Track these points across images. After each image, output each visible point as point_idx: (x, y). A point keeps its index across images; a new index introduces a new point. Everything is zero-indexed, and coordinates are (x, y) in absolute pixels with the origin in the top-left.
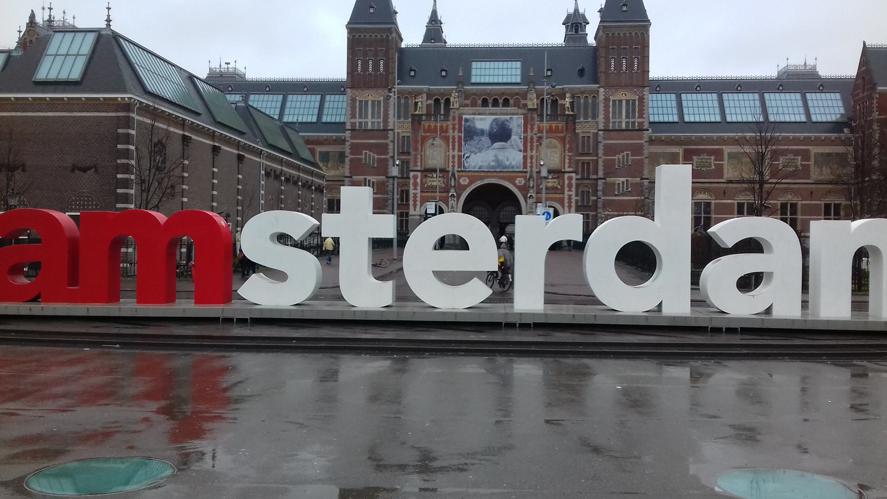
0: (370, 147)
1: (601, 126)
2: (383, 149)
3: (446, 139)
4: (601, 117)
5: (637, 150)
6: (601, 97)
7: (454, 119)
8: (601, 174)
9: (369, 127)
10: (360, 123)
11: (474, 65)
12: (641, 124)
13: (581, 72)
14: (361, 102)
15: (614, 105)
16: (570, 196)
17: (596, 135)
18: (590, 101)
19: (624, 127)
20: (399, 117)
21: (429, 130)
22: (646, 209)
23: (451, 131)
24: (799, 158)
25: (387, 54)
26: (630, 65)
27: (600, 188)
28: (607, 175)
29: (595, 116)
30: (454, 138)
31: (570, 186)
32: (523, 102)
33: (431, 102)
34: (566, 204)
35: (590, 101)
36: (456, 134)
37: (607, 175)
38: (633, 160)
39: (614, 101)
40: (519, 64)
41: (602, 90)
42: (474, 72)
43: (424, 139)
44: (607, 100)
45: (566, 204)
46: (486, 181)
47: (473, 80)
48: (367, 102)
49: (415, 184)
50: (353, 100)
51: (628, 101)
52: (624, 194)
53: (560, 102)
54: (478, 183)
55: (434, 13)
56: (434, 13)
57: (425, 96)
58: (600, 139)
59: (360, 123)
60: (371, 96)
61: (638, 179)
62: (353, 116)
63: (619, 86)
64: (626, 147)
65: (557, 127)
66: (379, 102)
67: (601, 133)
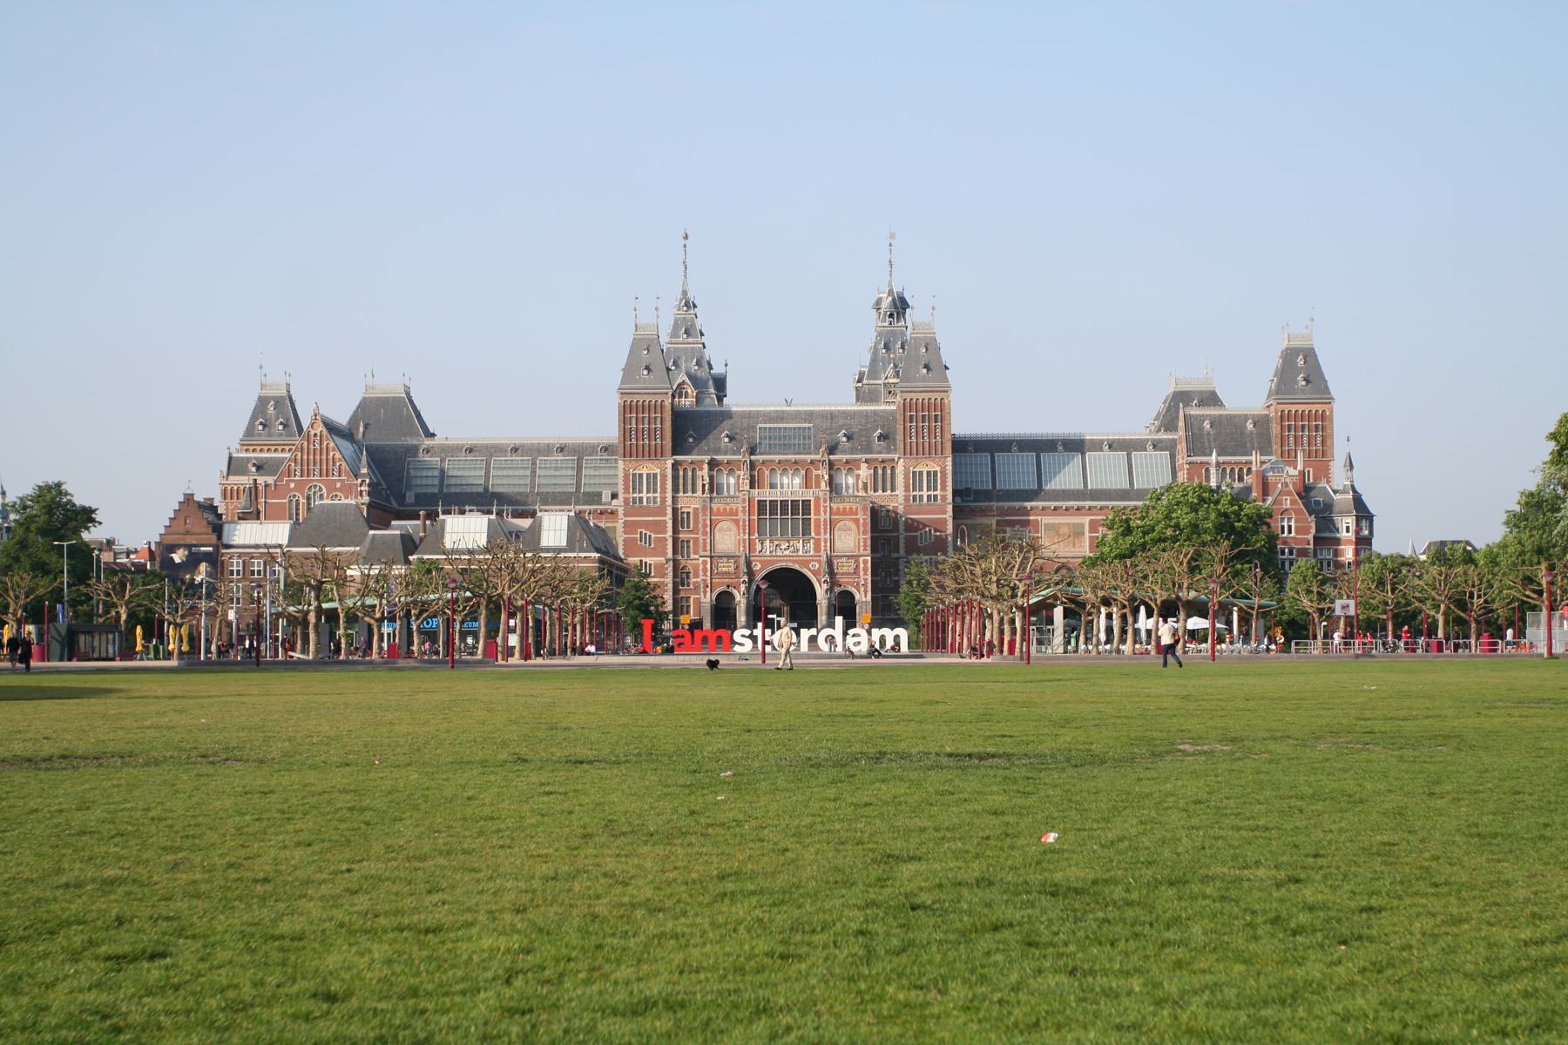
0: (647, 525)
1: (901, 499)
2: (660, 527)
3: (737, 522)
4: (900, 491)
6: (900, 469)
8: (902, 552)
12: (944, 498)
20: (675, 490)
28: (909, 552)
29: (893, 490)
31: (865, 569)
37: (909, 552)
46: (778, 566)
48: (641, 475)
49: (705, 570)
50: (626, 477)
54: (770, 568)
55: (685, 293)
56: (685, 293)
60: (646, 468)
62: (626, 490)
66: (655, 475)
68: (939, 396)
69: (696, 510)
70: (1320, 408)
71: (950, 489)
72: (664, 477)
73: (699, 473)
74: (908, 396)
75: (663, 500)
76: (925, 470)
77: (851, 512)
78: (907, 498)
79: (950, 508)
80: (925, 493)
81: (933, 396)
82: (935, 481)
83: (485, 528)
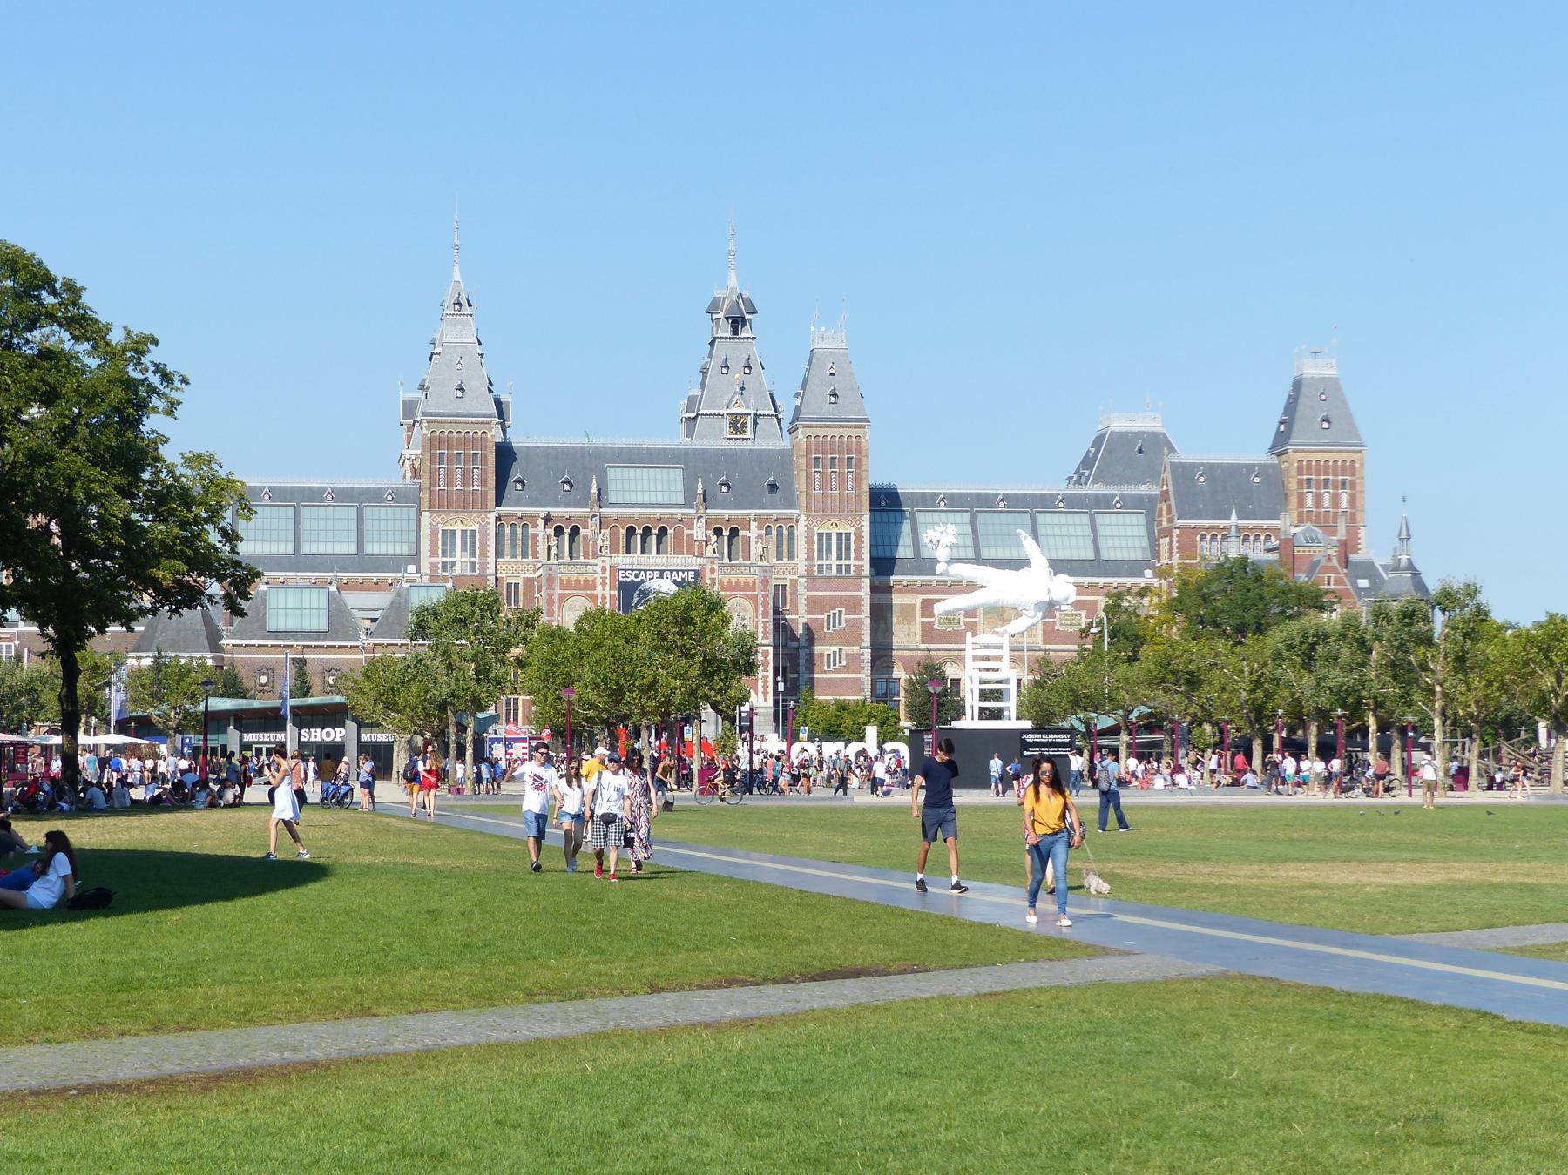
1: (802, 571)
4: (801, 559)
5: (853, 605)
6: (801, 530)
7: (604, 570)
9: (458, 570)
10: (444, 564)
11: (612, 473)
12: (859, 568)
13: (773, 487)
14: (444, 532)
15: (820, 540)
16: (765, 678)
17: (794, 583)
18: (786, 533)
19: (834, 571)
20: (499, 553)
21: (568, 585)
22: (862, 739)
23: (599, 588)
24: (1084, 613)
25: (484, 458)
26: (842, 481)
27: (802, 661)
29: (791, 557)
30: (604, 596)
32: (687, 532)
33: (552, 531)
34: (760, 690)
35: (786, 533)
36: (607, 592)
38: (847, 621)
39: (820, 535)
40: (679, 474)
41: (803, 518)
42: (611, 486)
43: (562, 599)
44: (810, 532)
45: (760, 690)
47: (612, 499)
48: (453, 532)
50: (434, 532)
51: (839, 535)
52: (836, 671)
53: (741, 533)
57: (541, 522)
58: (801, 589)
59: (444, 564)
60: (459, 524)
61: (856, 649)
62: (433, 553)
63: (825, 514)
64: (840, 601)
65: (747, 582)
66: (473, 533)
67: (803, 580)
68: (853, 432)
69: (528, 582)
70: (1348, 458)
71: (866, 556)
72: (484, 534)
73: (531, 531)
74: (813, 432)
75: (484, 565)
76: (834, 531)
77: (748, 586)
78: (810, 568)
79: (867, 583)
80: (834, 561)
81: (846, 432)
82: (848, 549)
83: (324, 604)
